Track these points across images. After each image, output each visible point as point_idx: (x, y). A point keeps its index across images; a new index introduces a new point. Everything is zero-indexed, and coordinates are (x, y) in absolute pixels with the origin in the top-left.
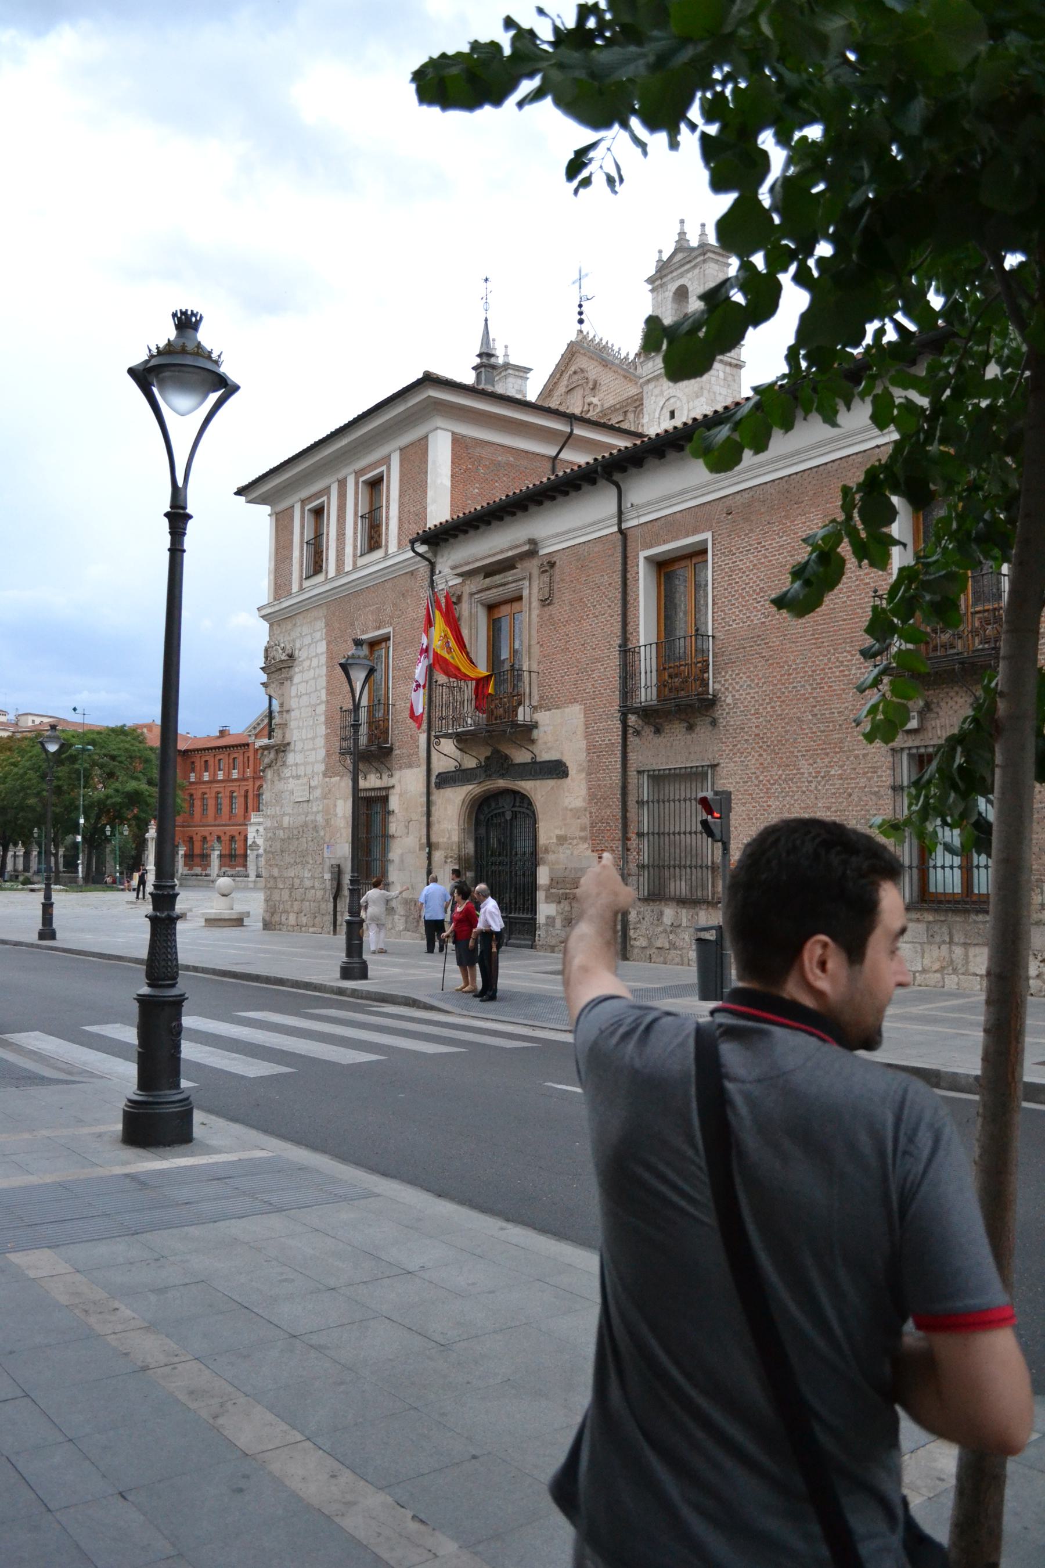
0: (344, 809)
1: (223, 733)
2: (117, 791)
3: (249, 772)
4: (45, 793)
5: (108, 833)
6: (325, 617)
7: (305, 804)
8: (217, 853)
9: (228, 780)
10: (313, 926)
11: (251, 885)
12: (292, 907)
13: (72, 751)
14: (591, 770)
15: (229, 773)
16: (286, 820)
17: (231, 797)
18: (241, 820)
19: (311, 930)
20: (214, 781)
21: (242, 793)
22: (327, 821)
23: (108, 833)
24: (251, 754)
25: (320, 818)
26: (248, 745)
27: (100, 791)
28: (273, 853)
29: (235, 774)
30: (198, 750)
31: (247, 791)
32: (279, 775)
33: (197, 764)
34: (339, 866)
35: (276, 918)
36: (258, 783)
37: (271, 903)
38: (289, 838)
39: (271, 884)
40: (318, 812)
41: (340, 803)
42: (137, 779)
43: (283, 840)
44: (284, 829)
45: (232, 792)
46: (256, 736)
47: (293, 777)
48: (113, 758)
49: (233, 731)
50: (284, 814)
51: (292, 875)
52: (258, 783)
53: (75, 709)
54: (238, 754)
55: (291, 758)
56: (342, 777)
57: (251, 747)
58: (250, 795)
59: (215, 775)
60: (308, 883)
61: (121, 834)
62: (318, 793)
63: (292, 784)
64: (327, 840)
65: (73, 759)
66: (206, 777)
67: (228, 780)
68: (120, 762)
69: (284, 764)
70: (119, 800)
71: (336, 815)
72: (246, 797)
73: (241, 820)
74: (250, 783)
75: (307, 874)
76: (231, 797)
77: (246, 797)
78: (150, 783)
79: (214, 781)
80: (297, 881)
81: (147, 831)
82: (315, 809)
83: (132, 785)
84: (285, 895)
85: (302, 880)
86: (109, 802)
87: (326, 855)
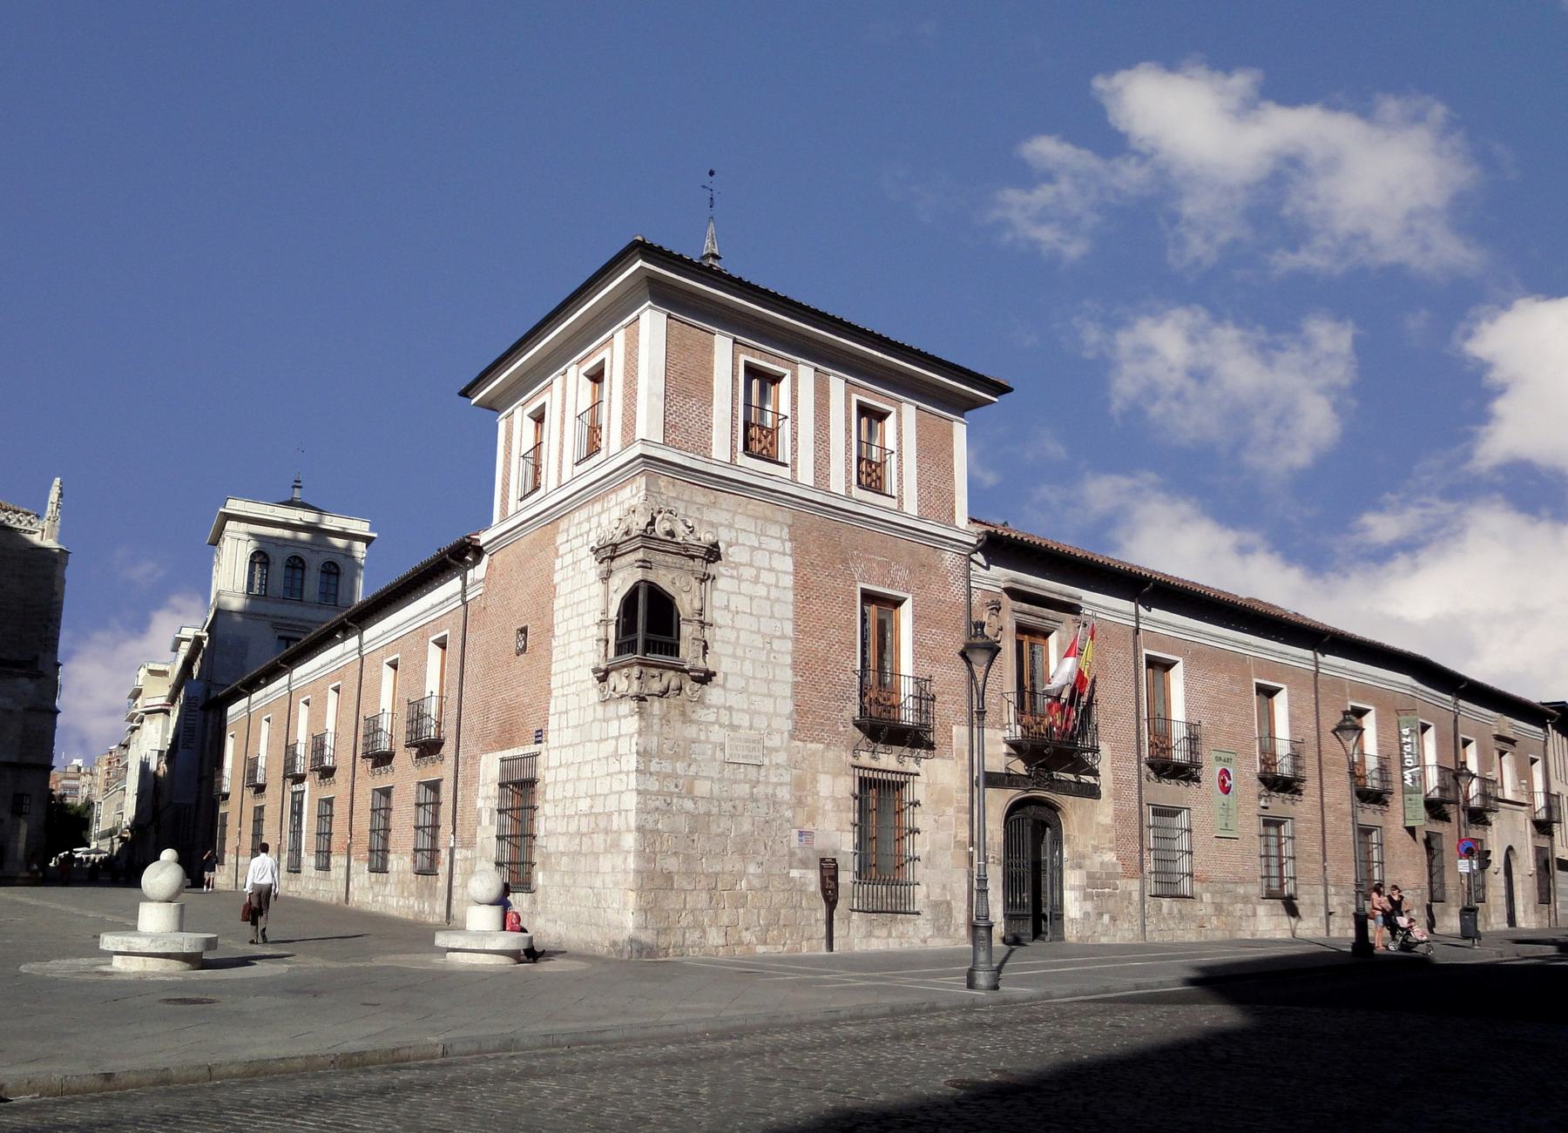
6: (790, 526)
7: (755, 769)
14: (1117, 795)
32: (683, 714)
38: (708, 814)
50: (696, 777)
55: (713, 693)
64: (798, 823)
69: (701, 701)
75: (752, 869)
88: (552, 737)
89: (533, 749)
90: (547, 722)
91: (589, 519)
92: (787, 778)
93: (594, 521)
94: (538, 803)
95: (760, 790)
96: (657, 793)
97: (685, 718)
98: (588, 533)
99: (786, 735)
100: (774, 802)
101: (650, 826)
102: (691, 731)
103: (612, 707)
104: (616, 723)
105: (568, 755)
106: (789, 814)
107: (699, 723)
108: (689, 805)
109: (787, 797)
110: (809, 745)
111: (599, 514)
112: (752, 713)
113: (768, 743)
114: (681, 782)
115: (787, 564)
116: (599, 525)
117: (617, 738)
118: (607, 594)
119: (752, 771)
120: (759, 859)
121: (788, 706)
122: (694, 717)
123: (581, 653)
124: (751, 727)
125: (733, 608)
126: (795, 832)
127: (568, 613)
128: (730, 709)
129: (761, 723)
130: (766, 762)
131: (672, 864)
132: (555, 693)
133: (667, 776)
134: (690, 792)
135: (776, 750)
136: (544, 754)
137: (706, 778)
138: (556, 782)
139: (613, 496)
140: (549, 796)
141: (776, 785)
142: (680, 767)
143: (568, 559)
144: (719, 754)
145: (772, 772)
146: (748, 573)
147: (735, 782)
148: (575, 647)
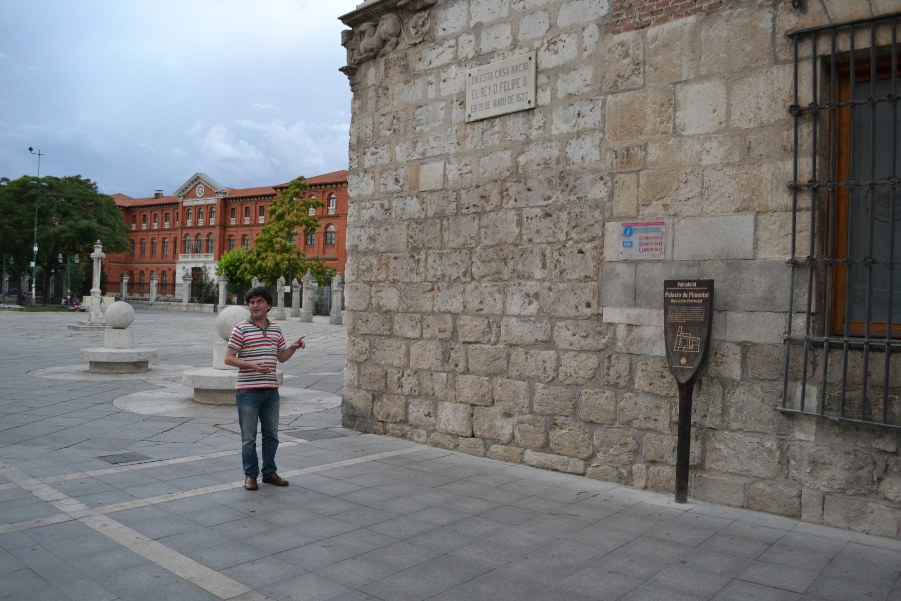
1: (157, 195)
2: (70, 227)
3: (178, 224)
4: (6, 226)
5: (60, 261)
7: (520, 120)
8: (155, 282)
9: (161, 229)
10: (545, 447)
11: (184, 309)
12: (451, 385)
13: (33, 192)
15: (162, 225)
16: (431, 175)
17: (163, 242)
18: (171, 259)
19: (530, 455)
20: (150, 230)
21: (172, 239)
23: (60, 261)
24: (180, 211)
25: (586, 152)
26: (177, 203)
27: (57, 226)
28: (379, 254)
29: (167, 225)
30: (138, 207)
31: (176, 239)
32: (406, 67)
33: (138, 217)
34: (708, 285)
35: (390, 407)
36: (185, 232)
37: (370, 369)
38: (441, 215)
39: (375, 323)
42: (87, 218)
43: (418, 222)
44: (420, 195)
45: (164, 239)
46: (184, 197)
47: (459, 62)
48: (69, 200)
49: (166, 194)
50: (424, 159)
51: (456, 305)
52: (185, 232)
53: (31, 149)
54: (170, 212)
56: (712, 10)
57: (180, 205)
58: (179, 241)
59: (151, 225)
60: (519, 331)
61: (73, 262)
62: (580, 80)
63: (455, 80)
65: (32, 199)
66: (144, 227)
67: (161, 229)
68: (75, 204)
70: (72, 234)
72: (175, 242)
73: (171, 259)
74: (179, 232)
75: (515, 305)
76: (163, 242)
77: (175, 242)
78: (101, 222)
79: (150, 230)
80: (471, 327)
81: (93, 251)
83: (83, 223)
84: (427, 355)
85: (494, 322)
86: (63, 236)
87: (610, 254)
92: (592, 118)
95: (534, 154)
96: (372, 198)
97: (409, 74)
100: (563, 177)
101: (362, 247)
102: (415, 92)
106: (598, 192)
107: (426, 73)
108: (413, 206)
109: (596, 155)
110: (651, 32)
113: (548, 60)
114: (402, 173)
119: (516, 128)
120: (531, 286)
122: (421, 67)
124: (515, 45)
126: (614, 229)
128: (479, 26)
129: (534, 29)
130: (545, 98)
131: (390, 298)
133: (384, 169)
134: (415, 186)
135: (567, 68)
137: (436, 158)
141: (565, 140)
142: (401, 152)
144: (457, 114)
145: (557, 117)
147: (485, 152)
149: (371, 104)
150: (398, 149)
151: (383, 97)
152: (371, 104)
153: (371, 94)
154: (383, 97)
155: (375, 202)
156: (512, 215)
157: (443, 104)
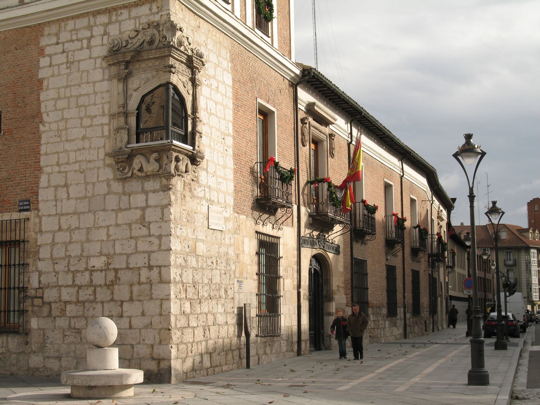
0: (250, 246)
7: (219, 233)
22: (237, 256)
40: (230, 245)
41: (246, 240)
71: (243, 251)
82: (227, 241)
88: (46, 206)
89: (16, 216)
90: (37, 194)
91: (90, 28)
93: (98, 31)
94: (30, 261)
98: (89, 39)
99: (232, 209)
103: (135, 185)
104: (143, 197)
105: (73, 222)
107: (198, 198)
111: (106, 25)
112: (218, 191)
115: (228, 79)
116: (105, 33)
117: (143, 209)
118: (126, 90)
121: (231, 188)
123: (84, 138)
125: (209, 110)
127: (61, 104)
128: (209, 187)
132: (48, 170)
136: (34, 220)
138: (53, 244)
139: (125, 12)
140: (44, 253)
143: (62, 59)
146: (215, 84)
148: (76, 133)
149: (179, 200)
150: (189, 231)
151: (183, 200)
152: (179, 200)
153: (179, 195)
154: (183, 200)
155: (182, 256)
156: (218, 272)
157: (202, 216)
